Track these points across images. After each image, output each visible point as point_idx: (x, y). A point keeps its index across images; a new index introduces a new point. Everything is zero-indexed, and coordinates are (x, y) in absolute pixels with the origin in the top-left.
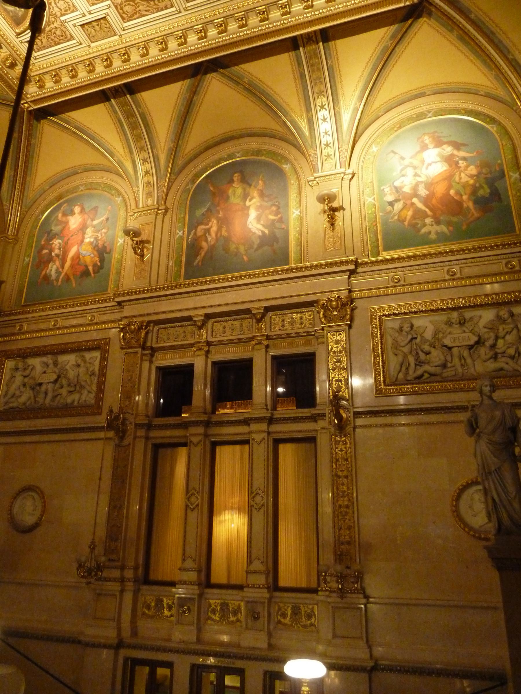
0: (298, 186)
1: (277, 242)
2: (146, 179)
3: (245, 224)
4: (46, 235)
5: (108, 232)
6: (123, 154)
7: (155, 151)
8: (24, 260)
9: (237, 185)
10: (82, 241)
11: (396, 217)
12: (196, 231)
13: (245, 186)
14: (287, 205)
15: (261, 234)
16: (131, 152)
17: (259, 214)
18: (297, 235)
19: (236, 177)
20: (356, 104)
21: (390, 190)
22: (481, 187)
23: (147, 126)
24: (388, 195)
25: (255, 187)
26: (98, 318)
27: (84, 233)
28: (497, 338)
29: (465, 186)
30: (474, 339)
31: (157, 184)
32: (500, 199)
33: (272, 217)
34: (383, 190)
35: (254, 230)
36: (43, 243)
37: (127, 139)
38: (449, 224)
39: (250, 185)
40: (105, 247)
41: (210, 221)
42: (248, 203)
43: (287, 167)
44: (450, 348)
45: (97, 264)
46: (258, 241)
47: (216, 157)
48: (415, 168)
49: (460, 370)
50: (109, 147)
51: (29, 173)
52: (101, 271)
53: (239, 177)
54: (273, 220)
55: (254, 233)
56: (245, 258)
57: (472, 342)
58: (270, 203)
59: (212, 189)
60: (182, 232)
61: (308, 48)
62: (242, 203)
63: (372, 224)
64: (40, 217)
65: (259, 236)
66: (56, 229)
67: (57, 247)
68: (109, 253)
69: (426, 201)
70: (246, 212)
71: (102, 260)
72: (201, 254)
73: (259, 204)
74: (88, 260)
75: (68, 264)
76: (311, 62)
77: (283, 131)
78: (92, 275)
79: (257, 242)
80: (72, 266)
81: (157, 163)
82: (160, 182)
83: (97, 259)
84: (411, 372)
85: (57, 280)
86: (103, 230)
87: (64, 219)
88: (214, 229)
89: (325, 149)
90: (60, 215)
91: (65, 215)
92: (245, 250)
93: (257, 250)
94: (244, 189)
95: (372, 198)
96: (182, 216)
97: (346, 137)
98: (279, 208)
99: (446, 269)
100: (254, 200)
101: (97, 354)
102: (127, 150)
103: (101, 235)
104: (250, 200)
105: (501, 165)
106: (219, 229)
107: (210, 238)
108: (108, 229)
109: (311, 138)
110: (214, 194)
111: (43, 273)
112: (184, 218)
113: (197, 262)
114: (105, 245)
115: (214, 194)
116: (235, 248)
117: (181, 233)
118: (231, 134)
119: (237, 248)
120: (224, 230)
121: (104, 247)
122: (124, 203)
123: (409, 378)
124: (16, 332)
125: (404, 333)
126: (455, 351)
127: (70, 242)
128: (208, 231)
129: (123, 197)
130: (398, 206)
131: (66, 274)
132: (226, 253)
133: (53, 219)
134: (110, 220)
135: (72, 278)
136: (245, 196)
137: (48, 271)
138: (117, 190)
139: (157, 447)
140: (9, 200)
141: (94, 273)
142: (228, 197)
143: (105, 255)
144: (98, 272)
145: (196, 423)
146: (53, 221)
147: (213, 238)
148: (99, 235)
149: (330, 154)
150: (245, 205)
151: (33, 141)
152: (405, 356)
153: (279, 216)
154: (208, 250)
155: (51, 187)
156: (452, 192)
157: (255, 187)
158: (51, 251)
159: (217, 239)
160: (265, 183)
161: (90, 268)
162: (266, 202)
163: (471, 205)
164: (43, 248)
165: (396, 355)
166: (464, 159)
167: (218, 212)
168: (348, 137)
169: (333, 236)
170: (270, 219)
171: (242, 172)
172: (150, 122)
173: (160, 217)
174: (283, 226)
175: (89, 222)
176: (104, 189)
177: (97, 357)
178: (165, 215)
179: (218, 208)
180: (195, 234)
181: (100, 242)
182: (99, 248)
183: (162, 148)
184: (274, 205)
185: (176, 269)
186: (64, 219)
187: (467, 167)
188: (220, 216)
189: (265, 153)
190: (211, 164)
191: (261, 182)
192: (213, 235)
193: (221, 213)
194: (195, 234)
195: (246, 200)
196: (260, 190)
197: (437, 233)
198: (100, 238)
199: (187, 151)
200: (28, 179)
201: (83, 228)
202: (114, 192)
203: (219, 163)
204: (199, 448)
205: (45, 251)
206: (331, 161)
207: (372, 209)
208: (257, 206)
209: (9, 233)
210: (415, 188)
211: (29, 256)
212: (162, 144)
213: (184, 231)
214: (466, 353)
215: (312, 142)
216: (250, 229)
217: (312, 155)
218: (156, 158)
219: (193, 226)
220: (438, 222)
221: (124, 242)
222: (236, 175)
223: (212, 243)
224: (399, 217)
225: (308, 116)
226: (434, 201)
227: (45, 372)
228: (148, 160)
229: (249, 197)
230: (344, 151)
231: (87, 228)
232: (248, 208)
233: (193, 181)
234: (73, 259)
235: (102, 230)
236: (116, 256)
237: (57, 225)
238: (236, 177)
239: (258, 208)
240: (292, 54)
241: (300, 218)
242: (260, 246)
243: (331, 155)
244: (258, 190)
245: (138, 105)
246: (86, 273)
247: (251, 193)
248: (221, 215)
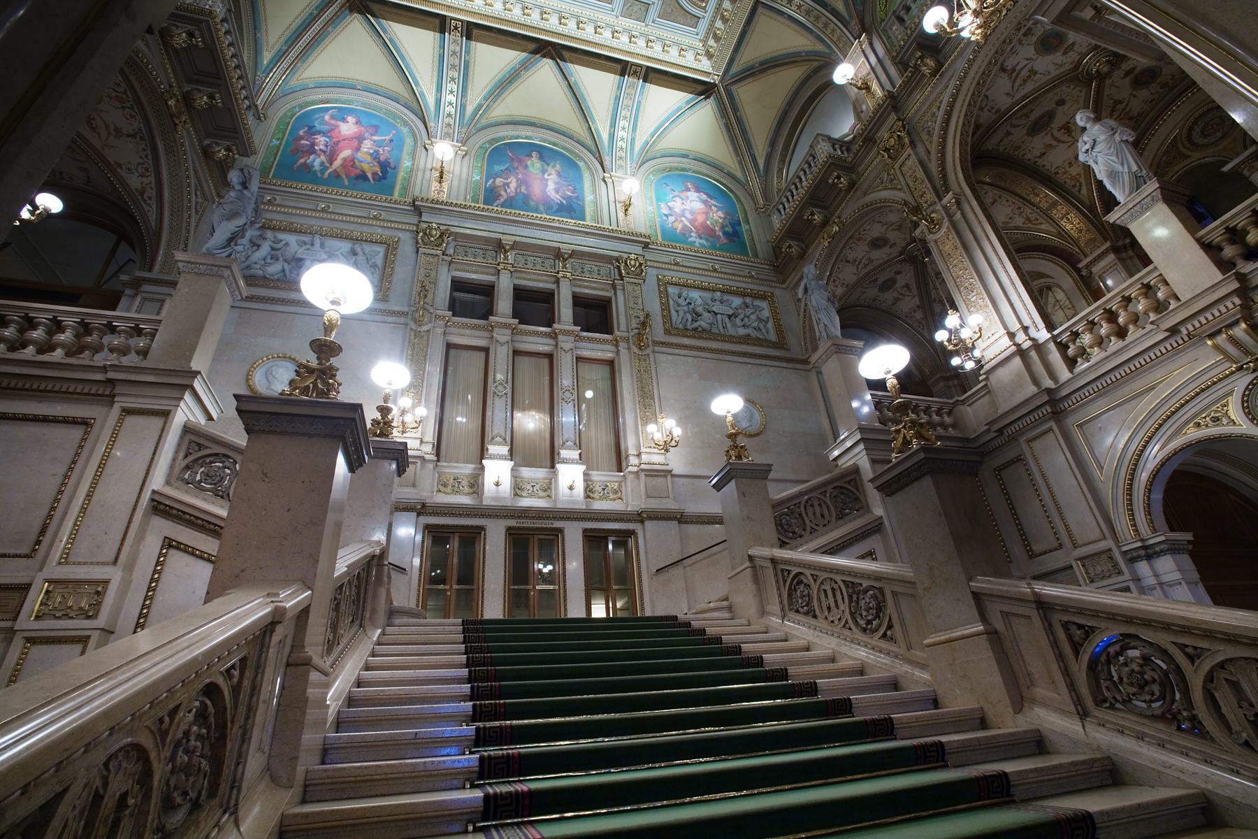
2: (447, 120)
3: (544, 191)
4: (306, 128)
7: (464, 100)
8: (271, 141)
10: (358, 149)
13: (543, 163)
14: (582, 189)
19: (534, 154)
22: (726, 226)
23: (466, 75)
26: (384, 215)
27: (360, 143)
28: (745, 316)
29: (716, 221)
30: (731, 312)
32: (739, 237)
36: (301, 133)
38: (707, 240)
39: (548, 165)
40: (390, 163)
42: (546, 176)
43: (581, 164)
44: (716, 314)
45: (378, 174)
47: (515, 133)
48: (682, 199)
49: (722, 331)
52: (383, 181)
57: (730, 313)
58: (566, 183)
61: (630, 79)
64: (297, 109)
66: (318, 126)
67: (322, 143)
68: (395, 168)
69: (692, 222)
74: (366, 167)
75: (337, 163)
80: (344, 166)
83: (377, 169)
84: (689, 323)
85: (323, 172)
87: (333, 122)
88: (513, 185)
90: (327, 117)
99: (711, 264)
100: (551, 177)
101: (381, 250)
104: (548, 175)
105: (738, 217)
106: (519, 186)
108: (393, 149)
110: (512, 160)
111: (302, 161)
115: (512, 160)
117: (478, 178)
118: (533, 120)
123: (689, 327)
125: (682, 298)
126: (719, 316)
127: (340, 145)
128: (508, 184)
129: (411, 128)
131: (335, 171)
133: (317, 116)
134: (395, 142)
135: (344, 176)
136: (544, 171)
137: (308, 161)
138: (403, 120)
139: (449, 346)
140: (266, 73)
141: (374, 180)
142: (526, 167)
145: (506, 326)
146: (317, 119)
151: (330, 29)
152: (685, 313)
155: (316, 87)
156: (708, 222)
158: (313, 145)
159: (516, 193)
161: (369, 175)
163: (721, 234)
164: (302, 138)
165: (677, 311)
166: (715, 206)
167: (517, 174)
172: (471, 73)
173: (459, 158)
175: (367, 135)
177: (379, 252)
178: (463, 157)
180: (494, 182)
186: (333, 122)
187: (717, 212)
194: (494, 182)
197: (700, 243)
201: (360, 139)
204: (505, 348)
210: (684, 210)
214: (727, 320)
219: (491, 175)
220: (701, 238)
221: (413, 165)
226: (696, 224)
227: (308, 249)
231: (365, 139)
233: (491, 142)
234: (345, 160)
236: (401, 174)
237: (321, 124)
239: (557, 183)
240: (618, 77)
241: (596, 203)
245: (468, 52)
246: (362, 177)
248: (520, 176)
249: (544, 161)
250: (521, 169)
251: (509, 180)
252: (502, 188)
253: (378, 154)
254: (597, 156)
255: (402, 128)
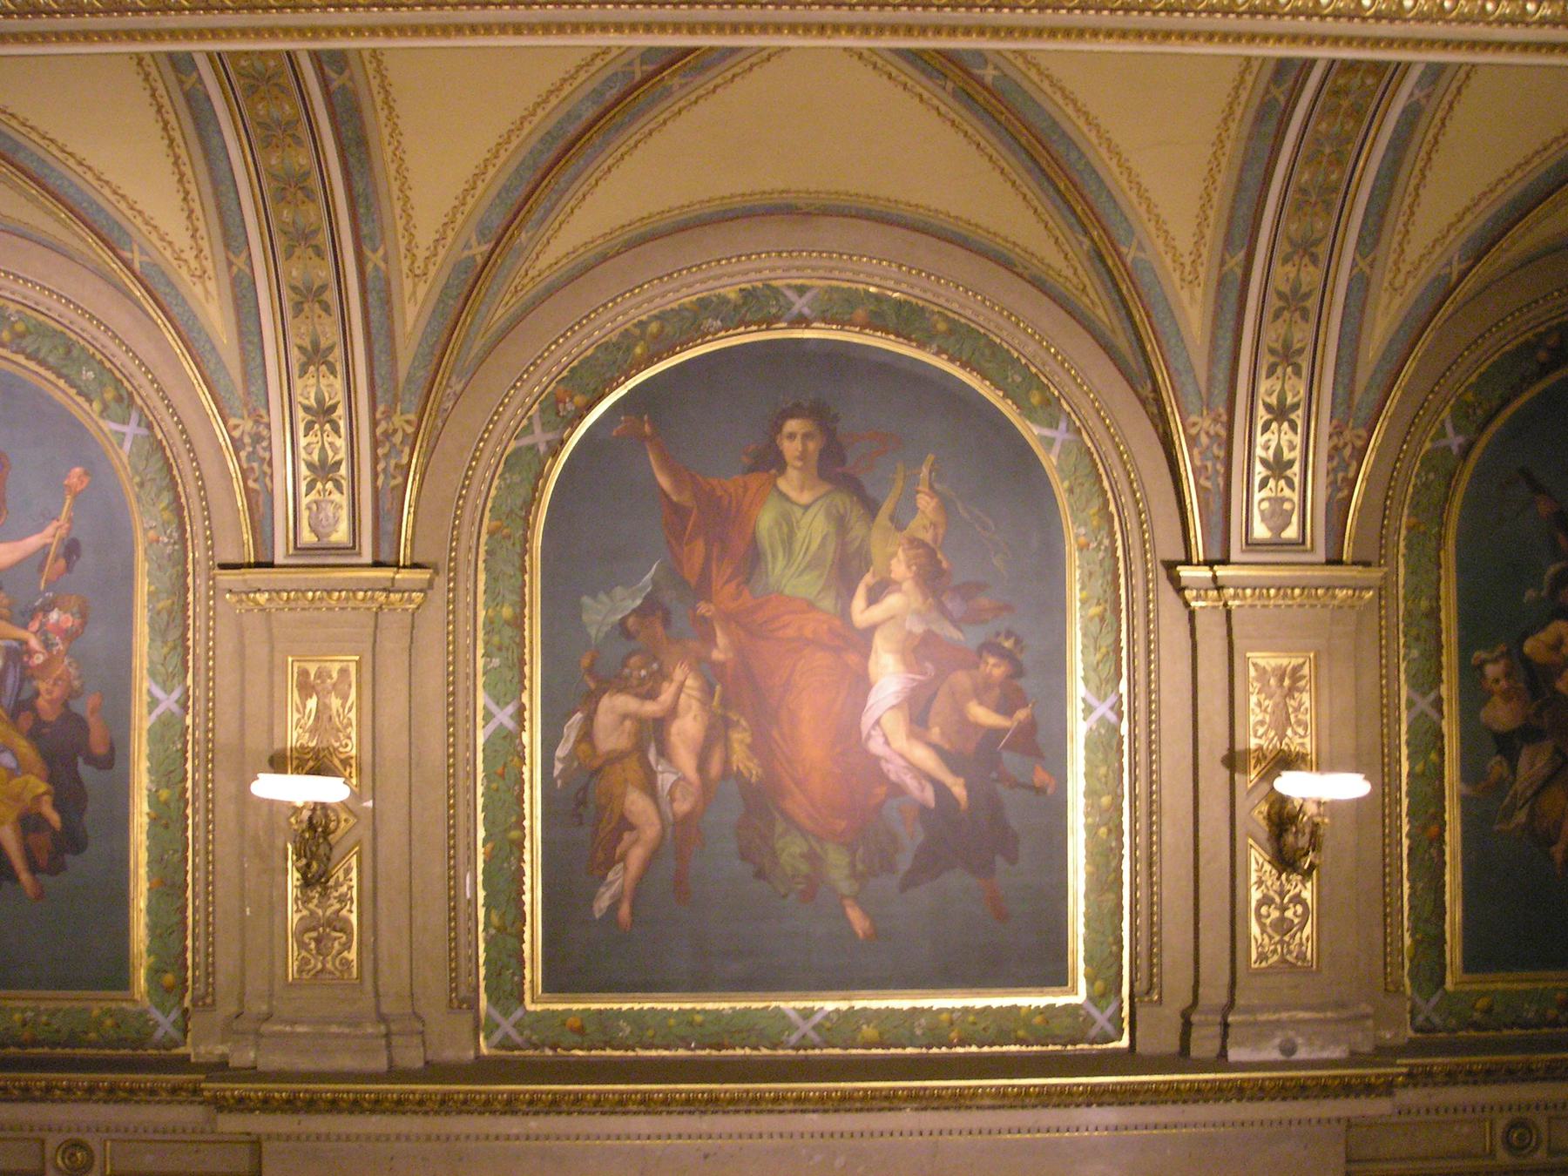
0: (1107, 563)
1: (1012, 859)
3: (848, 735)
5: (84, 624)
6: (183, 240)
7: (374, 259)
9: (802, 489)
11: (1521, 816)
12: (590, 719)
13: (842, 501)
15: (929, 796)
16: (232, 237)
17: (921, 685)
18: (1103, 831)
19: (796, 438)
20: (1449, 263)
21: (1508, 675)
24: (1496, 699)
25: (899, 524)
31: (374, 424)
33: (983, 715)
34: (1481, 666)
35: (895, 770)
37: (221, 182)
39: (871, 508)
40: (81, 724)
41: (662, 675)
42: (861, 613)
46: (921, 837)
50: (104, 198)
52: (69, 859)
53: (812, 446)
54: (994, 734)
55: (898, 790)
56: (858, 920)
59: (664, 481)
60: (511, 709)
62: (828, 603)
63: (1425, 828)
65: (923, 809)
70: (852, 659)
71: (69, 795)
72: (623, 858)
73: (918, 629)
76: (1341, 81)
77: (1069, 273)
78: (25, 877)
79: (911, 838)
81: (375, 315)
82: (388, 415)
86: (54, 616)
88: (688, 728)
89: (1266, 428)
92: (854, 875)
93: (909, 882)
94: (841, 524)
95: (1432, 696)
96: (507, 612)
97: (1367, 389)
98: (1018, 671)
100: (893, 602)
102: (209, 227)
103: (47, 645)
104: (873, 598)
107: (673, 778)
108: (83, 615)
109: (1212, 362)
112: (518, 623)
113: (603, 903)
114: (78, 707)
116: (803, 856)
119: (812, 857)
120: (740, 738)
121: (73, 722)
122: (156, 463)
128: (654, 732)
130: (1532, 765)
132: (760, 874)
134: (87, 559)
138: (109, 375)
141: (34, 868)
142: (753, 559)
143: (86, 771)
144: (55, 867)
147: (683, 779)
148: (34, 643)
149: (1287, 456)
150: (845, 614)
153: (1021, 714)
154: (662, 837)
157: (899, 524)
159: (707, 788)
160: (945, 505)
162: (956, 623)
167: (709, 639)
168: (1374, 395)
169: (1282, 894)
170: (977, 726)
171: (821, 416)
174: (1040, 777)
176: (29, 344)
179: (704, 608)
180: (587, 735)
181: (42, 686)
182: (39, 722)
183: (421, 253)
184: (989, 647)
185: (495, 919)
188: (717, 655)
189: (942, 326)
190: (654, 327)
191: (926, 502)
192: (686, 761)
193: (721, 639)
194: (587, 735)
195: (851, 593)
196: (922, 544)
198: (39, 659)
199: (543, 263)
202: (91, 375)
203: (700, 335)
206: (1287, 492)
207: (1427, 753)
208: (910, 633)
212: (425, 238)
213: (522, 708)
215: (1211, 380)
216: (876, 760)
217: (1204, 440)
218: (379, 297)
222: (792, 425)
223: (682, 807)
224: (1532, 815)
225: (1223, 263)
228: (331, 296)
229: (868, 579)
230: (1347, 452)
232: (863, 640)
235: (47, 608)
238: (796, 438)
242: (930, 862)
243: (1291, 463)
244: (915, 543)
247: (876, 552)
248: (721, 651)
249: (850, 484)
250: (725, 592)
251: (667, 693)
252: (632, 764)
253: (27, 675)
254: (1147, 391)
255: (109, 426)
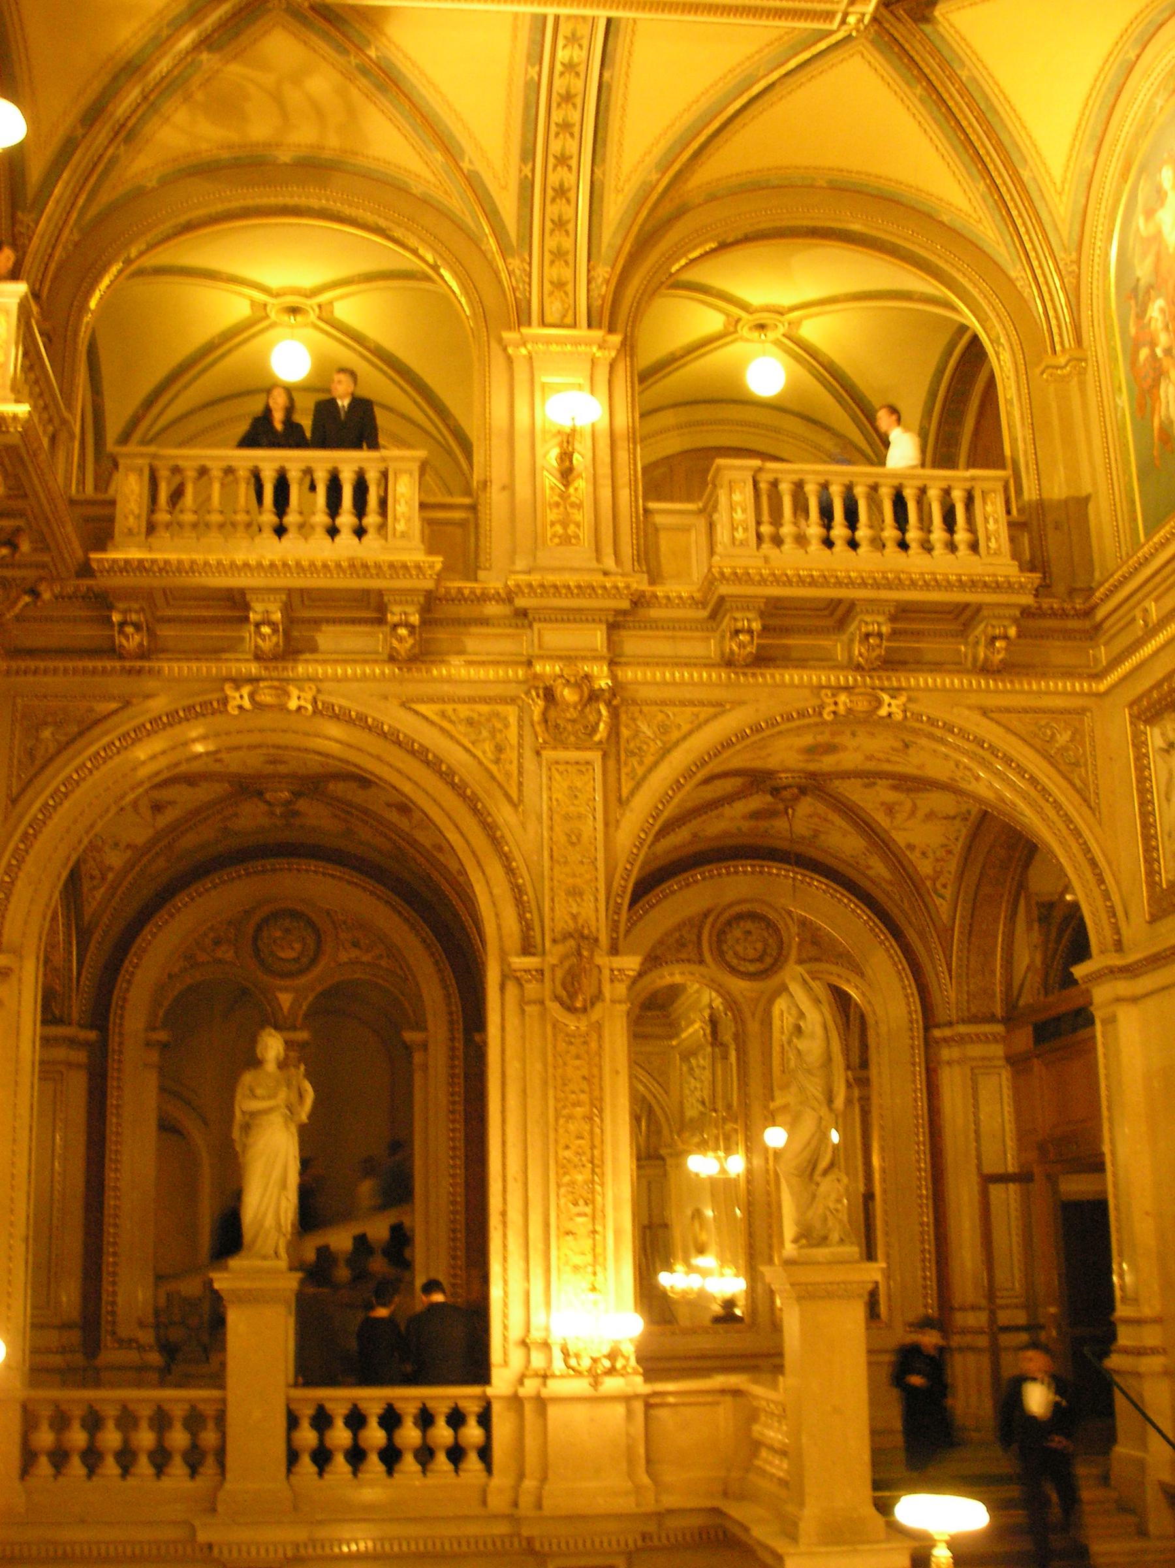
4: (1133, 303)
36: (1133, 330)
51: (1015, 157)
66: (1143, 271)
90: (1141, 220)
91: (1150, 214)
124: (1140, 633)
151: (964, 74)
158: (1153, 345)
200: (1025, 175)
205: (1144, 353)
209: (1058, 348)
211: (1120, 389)
